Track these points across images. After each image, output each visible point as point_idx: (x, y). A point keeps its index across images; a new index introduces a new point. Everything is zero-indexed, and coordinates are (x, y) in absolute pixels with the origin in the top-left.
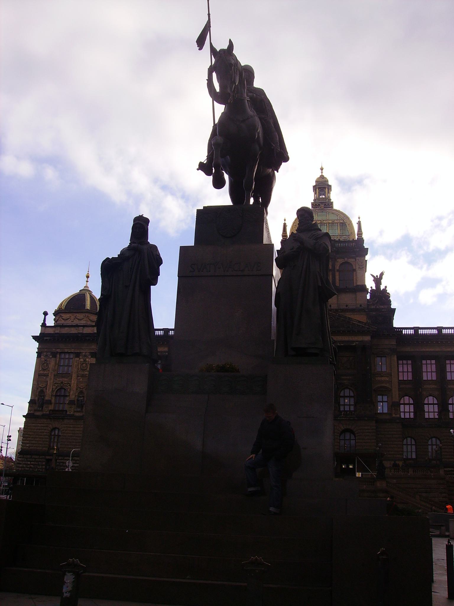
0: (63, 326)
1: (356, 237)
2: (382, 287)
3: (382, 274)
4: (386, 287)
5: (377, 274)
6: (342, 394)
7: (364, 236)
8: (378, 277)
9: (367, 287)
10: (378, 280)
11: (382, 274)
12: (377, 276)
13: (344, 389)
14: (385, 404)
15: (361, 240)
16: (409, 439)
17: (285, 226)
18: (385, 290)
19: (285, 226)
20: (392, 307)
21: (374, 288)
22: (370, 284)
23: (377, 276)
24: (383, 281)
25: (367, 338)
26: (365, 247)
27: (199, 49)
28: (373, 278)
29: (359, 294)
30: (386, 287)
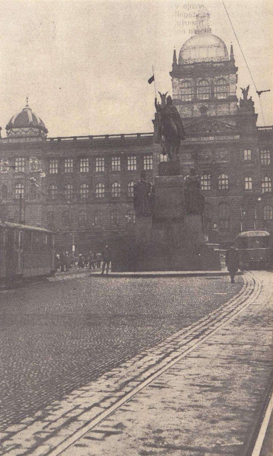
0: (12, 138)
1: (230, 58)
2: (248, 98)
3: (248, 88)
4: (251, 97)
5: (245, 87)
6: (219, 178)
7: (235, 58)
8: (245, 90)
9: (238, 98)
10: (245, 92)
11: (248, 88)
12: (245, 89)
13: (221, 174)
14: (251, 184)
15: (233, 60)
16: (268, 206)
17: (175, 51)
18: (250, 99)
19: (175, 51)
20: (256, 113)
21: (242, 98)
22: (240, 95)
23: (245, 89)
24: (249, 93)
25: (238, 137)
26: (236, 66)
27: (150, 84)
28: (241, 91)
29: (232, 104)
30: (251, 97)
